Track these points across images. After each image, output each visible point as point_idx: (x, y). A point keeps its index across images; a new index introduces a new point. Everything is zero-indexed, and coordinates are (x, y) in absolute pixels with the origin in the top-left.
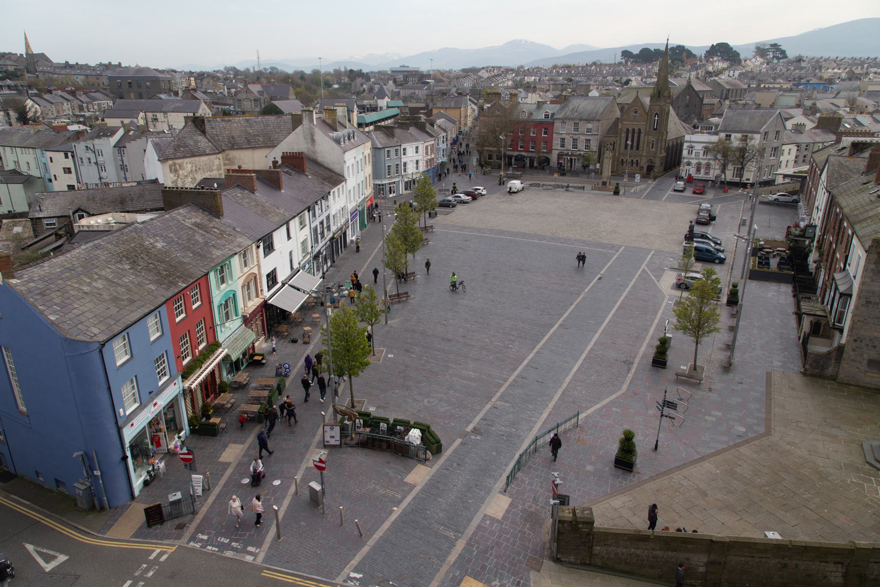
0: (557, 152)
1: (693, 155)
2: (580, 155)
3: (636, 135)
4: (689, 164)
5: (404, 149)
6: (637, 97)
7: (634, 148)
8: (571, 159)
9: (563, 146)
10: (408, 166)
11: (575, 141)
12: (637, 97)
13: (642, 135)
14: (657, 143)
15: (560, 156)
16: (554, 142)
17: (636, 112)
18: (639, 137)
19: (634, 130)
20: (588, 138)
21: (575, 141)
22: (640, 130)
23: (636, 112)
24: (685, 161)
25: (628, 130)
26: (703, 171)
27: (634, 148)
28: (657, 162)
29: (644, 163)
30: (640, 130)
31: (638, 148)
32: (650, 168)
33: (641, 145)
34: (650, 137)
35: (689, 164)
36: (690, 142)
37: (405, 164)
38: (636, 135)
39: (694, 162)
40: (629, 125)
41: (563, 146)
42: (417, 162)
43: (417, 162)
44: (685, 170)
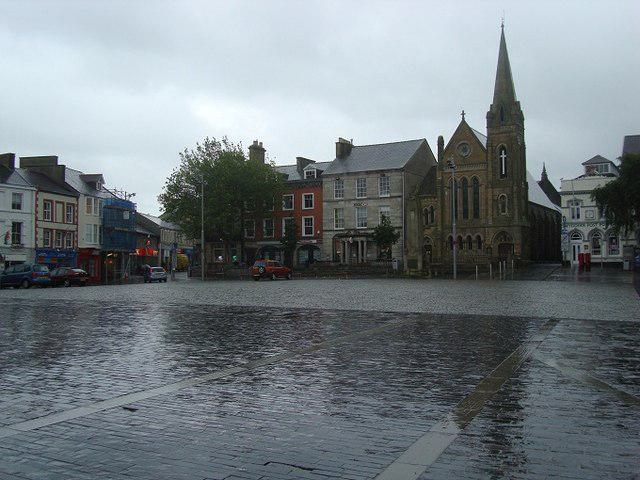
0: (333, 234)
1: (582, 219)
4: (576, 235)
6: (463, 121)
7: (470, 216)
8: (356, 244)
12: (463, 121)
13: (482, 190)
14: (511, 201)
16: (326, 217)
17: (465, 150)
18: (476, 193)
23: (465, 150)
24: (569, 229)
26: (604, 248)
27: (470, 216)
28: (517, 238)
29: (490, 239)
30: (475, 179)
31: (476, 215)
32: (505, 248)
33: (482, 208)
34: (497, 191)
35: (576, 235)
39: (586, 230)
44: (574, 248)
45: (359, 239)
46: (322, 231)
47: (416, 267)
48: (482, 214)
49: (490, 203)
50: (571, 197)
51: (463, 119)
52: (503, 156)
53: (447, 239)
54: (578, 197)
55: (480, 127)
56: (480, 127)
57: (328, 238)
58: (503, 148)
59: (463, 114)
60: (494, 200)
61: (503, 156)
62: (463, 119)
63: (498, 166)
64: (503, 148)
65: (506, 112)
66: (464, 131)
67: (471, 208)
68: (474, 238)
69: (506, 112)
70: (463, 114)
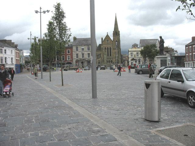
2: (86, 60)
3: (109, 50)
5: (5, 50)
7: (109, 56)
9: (77, 57)
10: (7, 60)
11: (83, 54)
15: (77, 61)
16: (74, 56)
17: (108, 41)
19: (108, 48)
20: (88, 53)
21: (83, 54)
22: (110, 48)
23: (108, 41)
25: (105, 48)
27: (109, 56)
30: (110, 48)
31: (110, 55)
33: (112, 54)
36: (131, 51)
37: (6, 58)
38: (109, 50)
40: (107, 46)
41: (77, 57)
42: (12, 58)
43: (12, 58)
45: (84, 61)
46: (73, 59)
48: (112, 55)
49: (114, 53)
50: (131, 52)
52: (117, 43)
54: (133, 52)
57: (74, 61)
58: (116, 41)
64: (116, 41)
65: (116, 33)
66: (107, 36)
67: (109, 54)
68: (110, 61)
69: (116, 33)
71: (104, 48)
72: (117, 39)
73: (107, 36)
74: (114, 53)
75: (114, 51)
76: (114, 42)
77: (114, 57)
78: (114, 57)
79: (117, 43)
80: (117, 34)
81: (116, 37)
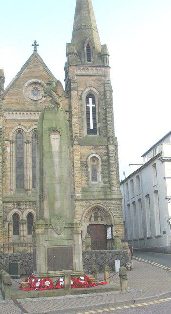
6: (35, 56)
12: (35, 56)
47: (69, 264)
49: (77, 165)
51: (35, 50)
53: (10, 217)
55: (57, 65)
56: (57, 65)
58: (90, 95)
59: (35, 45)
60: (81, 162)
61: (91, 105)
62: (35, 50)
63: (85, 117)
66: (35, 62)
70: (35, 45)
71: (12, 135)
72: (89, 84)
73: (35, 62)
74: (77, 165)
75: (77, 157)
76: (80, 98)
77: (79, 194)
78: (79, 194)
79: (91, 105)
80: (94, 57)
81: (91, 71)
